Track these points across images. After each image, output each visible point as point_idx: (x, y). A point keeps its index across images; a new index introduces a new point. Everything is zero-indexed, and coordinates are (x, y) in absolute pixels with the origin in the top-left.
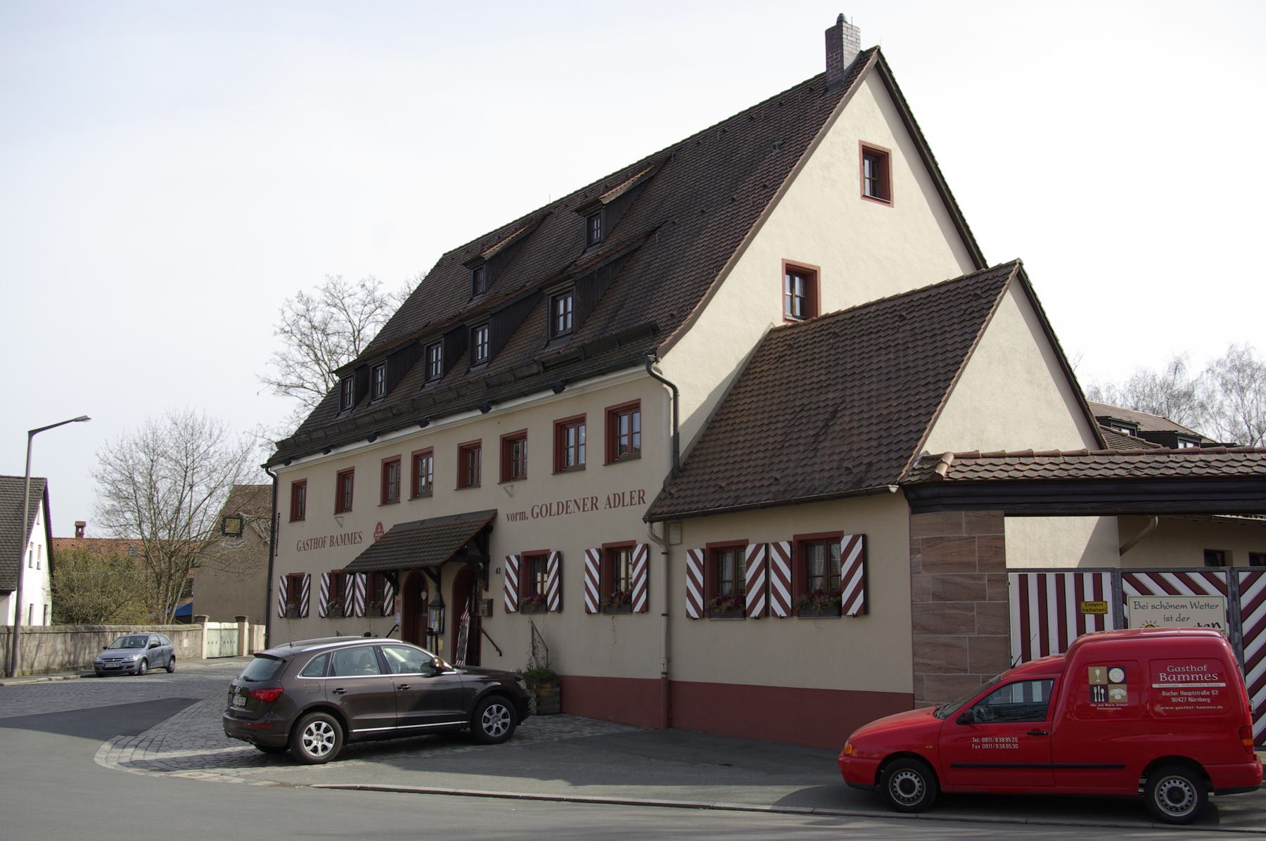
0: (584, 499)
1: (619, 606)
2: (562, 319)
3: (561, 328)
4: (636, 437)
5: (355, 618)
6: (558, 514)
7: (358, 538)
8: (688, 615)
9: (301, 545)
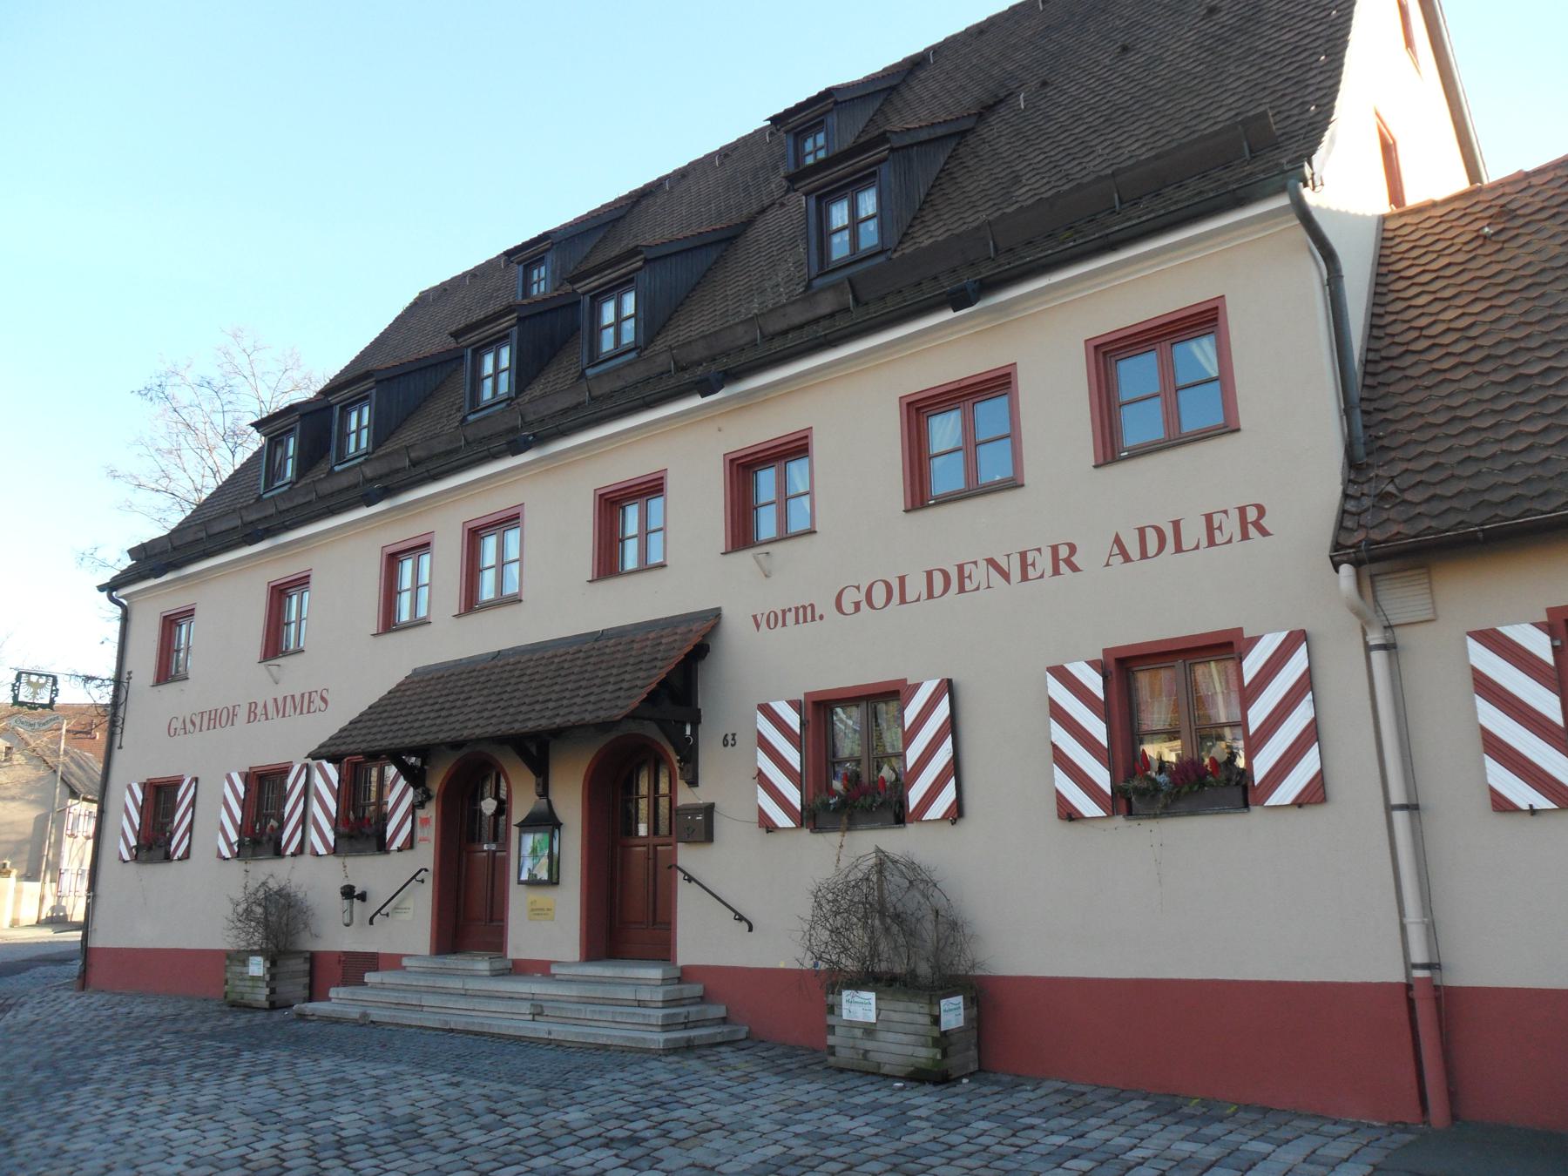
0: (310, 693)
1: (1166, 806)
2: (353, 437)
3: (352, 449)
4: (655, 541)
5: (307, 858)
6: (930, 596)
7: (318, 701)
8: (1501, 804)
9: (177, 724)
